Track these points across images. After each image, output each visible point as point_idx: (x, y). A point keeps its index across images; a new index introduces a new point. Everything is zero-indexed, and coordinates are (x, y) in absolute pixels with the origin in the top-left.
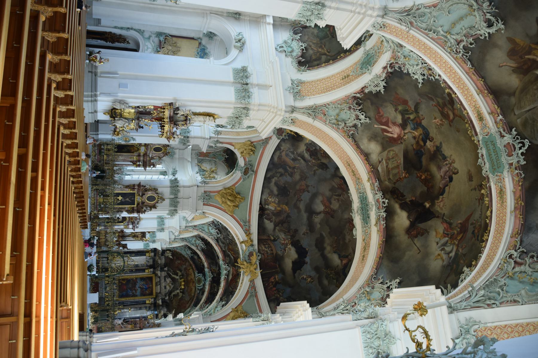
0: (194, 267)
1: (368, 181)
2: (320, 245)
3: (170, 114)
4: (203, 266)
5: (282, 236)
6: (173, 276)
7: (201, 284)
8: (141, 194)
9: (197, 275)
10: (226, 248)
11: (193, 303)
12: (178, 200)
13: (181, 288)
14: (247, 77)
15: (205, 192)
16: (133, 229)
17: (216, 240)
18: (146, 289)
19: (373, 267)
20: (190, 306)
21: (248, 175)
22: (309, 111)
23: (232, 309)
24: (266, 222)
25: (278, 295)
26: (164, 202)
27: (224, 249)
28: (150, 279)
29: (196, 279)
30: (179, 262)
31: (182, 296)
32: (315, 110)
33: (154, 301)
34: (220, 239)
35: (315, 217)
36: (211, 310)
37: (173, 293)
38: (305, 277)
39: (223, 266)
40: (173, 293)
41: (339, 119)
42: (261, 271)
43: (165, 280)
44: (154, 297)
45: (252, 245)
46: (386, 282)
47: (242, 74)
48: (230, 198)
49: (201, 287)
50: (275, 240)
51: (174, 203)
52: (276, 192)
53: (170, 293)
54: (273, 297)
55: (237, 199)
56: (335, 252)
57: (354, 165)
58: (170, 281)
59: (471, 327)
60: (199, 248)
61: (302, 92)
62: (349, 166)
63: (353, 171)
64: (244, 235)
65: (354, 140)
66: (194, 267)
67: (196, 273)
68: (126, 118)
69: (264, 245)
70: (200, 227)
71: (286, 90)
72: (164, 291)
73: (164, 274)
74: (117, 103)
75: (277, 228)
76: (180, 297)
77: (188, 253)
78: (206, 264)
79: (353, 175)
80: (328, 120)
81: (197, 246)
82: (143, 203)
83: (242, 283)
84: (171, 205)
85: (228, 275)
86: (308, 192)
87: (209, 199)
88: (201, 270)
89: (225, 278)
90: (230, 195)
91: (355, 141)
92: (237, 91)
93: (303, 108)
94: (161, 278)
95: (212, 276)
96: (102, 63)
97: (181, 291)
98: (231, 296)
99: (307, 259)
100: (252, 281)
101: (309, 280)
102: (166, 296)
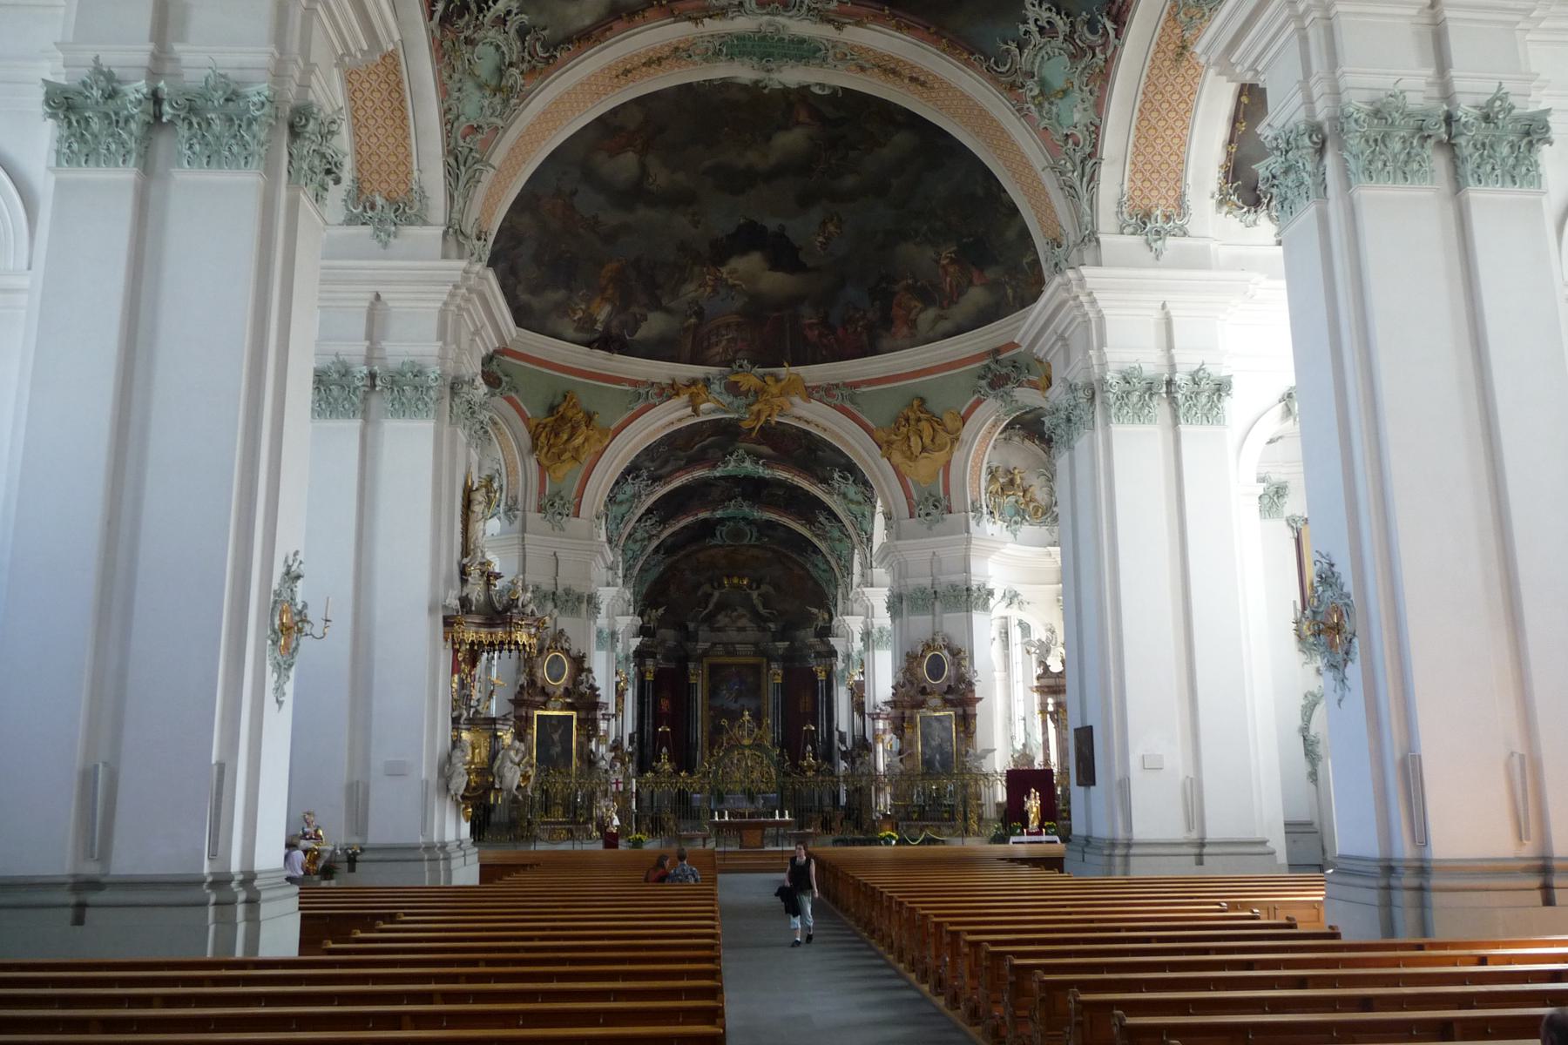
0: (694, 548)
1: (696, 20)
2: (735, 181)
3: (480, 625)
4: (705, 520)
5: (690, 290)
6: (711, 606)
7: (747, 529)
8: (539, 699)
9: (717, 541)
10: (682, 454)
12: (560, 591)
14: (346, 372)
15: (541, 509)
16: (609, 720)
17: (654, 481)
19: (967, 63)
20: (803, 567)
21: (500, 374)
22: (463, 179)
23: (883, 456)
24: (642, 333)
25: (861, 323)
26: (568, 633)
27: (683, 463)
28: (714, 670)
29: (728, 542)
32: (461, 159)
33: (777, 661)
34: (655, 470)
35: (655, 181)
36: (849, 510)
38: (821, 239)
39: (731, 467)
41: (493, 83)
42: (785, 364)
43: (719, 630)
44: (765, 660)
45: (707, 382)
46: (1022, 33)
47: (335, 390)
48: (565, 437)
49: (755, 530)
50: (699, 314)
51: (570, 604)
52: (559, 295)
53: (757, 617)
54: (865, 338)
55: (570, 414)
56: (769, 139)
57: (632, 57)
58: (726, 616)
60: (654, 532)
61: (394, 195)
62: (629, 71)
63: (648, 63)
64: (675, 402)
65: (562, 42)
66: (694, 548)
67: (714, 542)
68: (493, 756)
69: (709, 347)
70: (614, 526)
71: (385, 245)
72: (752, 634)
73: (703, 632)
74: (453, 786)
75: (665, 302)
76: (771, 590)
77: (652, 563)
78: (703, 515)
79: (660, 65)
80: (493, 119)
81: (650, 538)
82: (567, 692)
83: (808, 422)
84: (575, 611)
85: (757, 457)
86: (574, 193)
87: (562, 499)
88: (707, 527)
89: (764, 464)
90: (557, 435)
91: (568, 40)
92: (402, 409)
93: (452, 197)
94: (717, 641)
95: (740, 499)
96: (321, 833)
97: (754, 586)
98: (820, 453)
99: (772, 224)
100: (810, 393)
101: (831, 228)
102: (764, 630)
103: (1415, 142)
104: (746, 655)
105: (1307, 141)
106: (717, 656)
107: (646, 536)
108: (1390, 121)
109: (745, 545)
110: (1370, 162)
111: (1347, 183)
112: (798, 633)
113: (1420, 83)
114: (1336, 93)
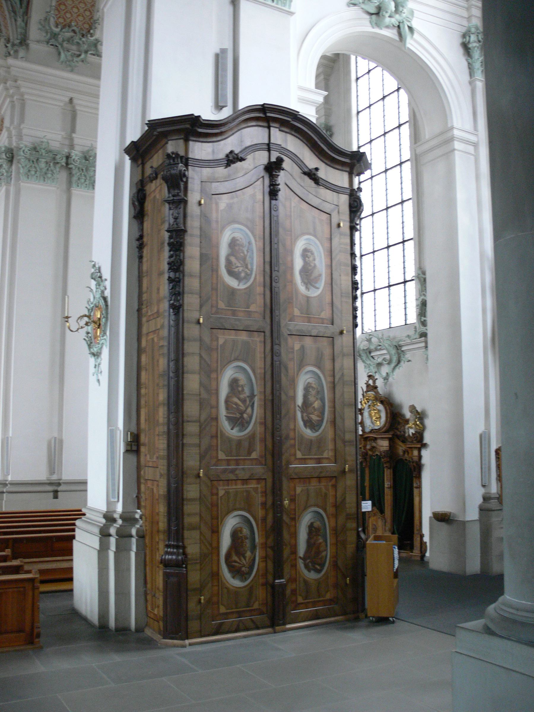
59: (51, 28)
103: (52, 164)
105: (4, 157)
108: (40, 153)
110: (29, 171)
111: (18, 179)
113: (59, 138)
114: (20, 137)
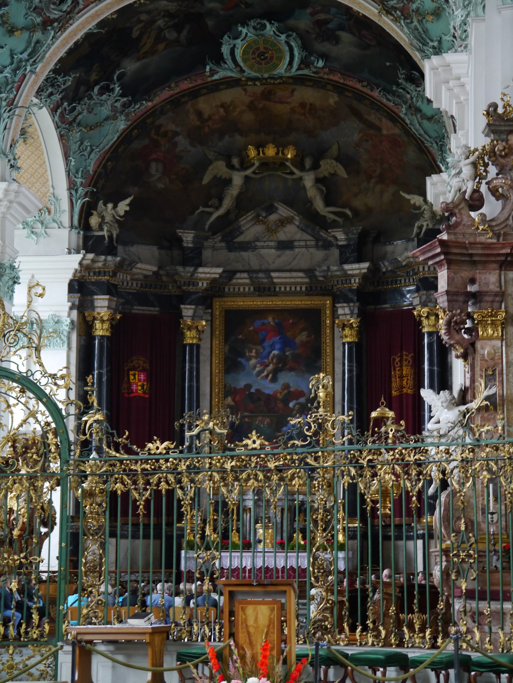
0: (185, 85)
6: (227, 203)
11: (376, 94)
13: (292, 160)
18: (286, 343)
30: (155, 169)
31: (337, 159)
33: (347, 300)
37: (319, 205)
40: (319, 205)
43: (246, 246)
58: (257, 220)
60: (55, 14)
66: (185, 85)
76: (342, 172)
77: (105, 111)
81: (47, 23)
94: (240, 267)
97: (308, 163)
102: (327, 245)
104: (295, 293)
106: (244, 295)
107: (39, 20)
109: (281, 77)
112: (389, 248)
